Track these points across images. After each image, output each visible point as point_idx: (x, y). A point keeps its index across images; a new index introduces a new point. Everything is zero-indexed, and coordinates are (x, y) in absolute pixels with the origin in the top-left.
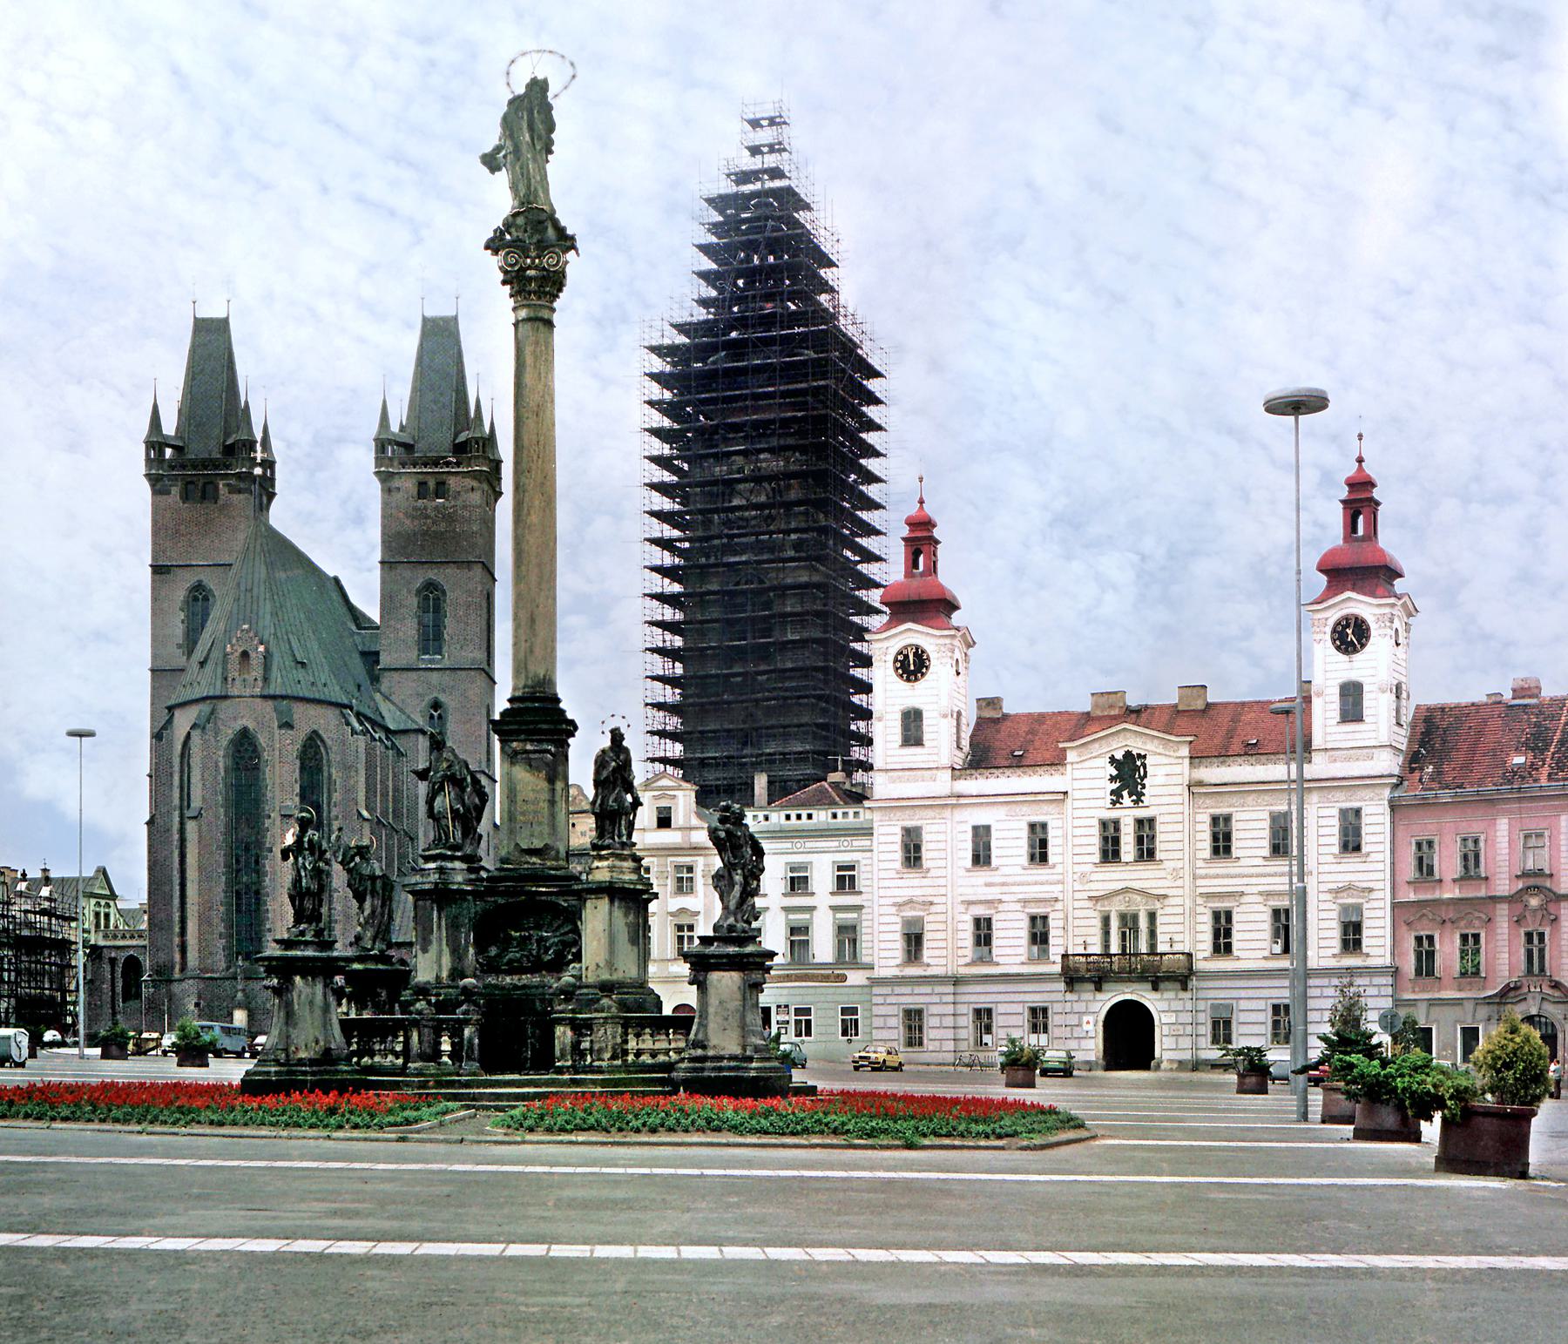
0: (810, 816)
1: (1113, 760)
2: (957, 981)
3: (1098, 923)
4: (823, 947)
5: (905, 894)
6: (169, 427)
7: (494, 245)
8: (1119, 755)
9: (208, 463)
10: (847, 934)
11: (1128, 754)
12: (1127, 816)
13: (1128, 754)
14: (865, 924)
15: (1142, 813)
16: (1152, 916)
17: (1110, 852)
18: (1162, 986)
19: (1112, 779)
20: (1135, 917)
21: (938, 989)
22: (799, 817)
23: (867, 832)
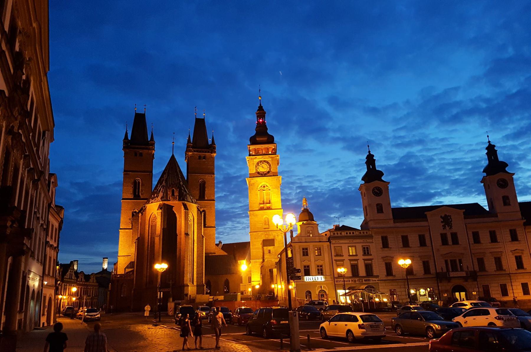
1: (441, 217)
3: (444, 262)
8: (443, 216)
11: (446, 215)
13: (446, 215)
17: (444, 242)
19: (442, 222)
20: (455, 261)
22: (350, 233)
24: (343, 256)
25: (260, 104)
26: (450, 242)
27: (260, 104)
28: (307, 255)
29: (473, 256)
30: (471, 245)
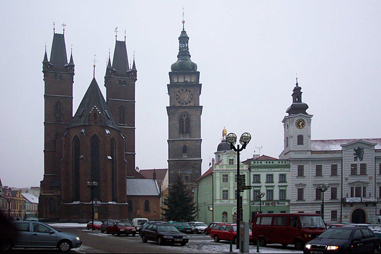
0: (273, 162)
14: (287, 190)
16: (364, 188)
17: (353, 172)
18: (369, 205)
20: (361, 187)
21: (308, 207)
22: (270, 162)
24: (261, 183)
26: (358, 172)
28: (227, 181)
29: (376, 184)
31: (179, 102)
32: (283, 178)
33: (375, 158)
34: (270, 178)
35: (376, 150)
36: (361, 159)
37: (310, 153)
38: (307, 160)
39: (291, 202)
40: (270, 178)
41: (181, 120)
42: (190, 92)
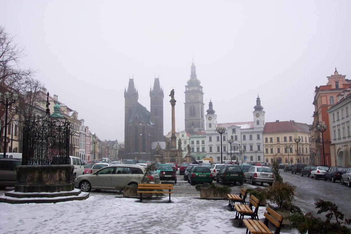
1: (232, 129)
2: (216, 154)
4: (201, 150)
5: (209, 144)
6: (127, 91)
7: (170, 102)
9: (131, 95)
10: (203, 148)
12: (234, 135)
15: (236, 135)
23: (205, 137)
25: (193, 62)
27: (193, 62)
29: (242, 145)
30: (242, 141)
31: (190, 100)
32: (203, 142)
33: (241, 133)
34: (198, 142)
35: (241, 129)
36: (235, 133)
37: (214, 131)
38: (213, 134)
39: (207, 153)
40: (198, 142)
41: (191, 110)
42: (194, 95)
